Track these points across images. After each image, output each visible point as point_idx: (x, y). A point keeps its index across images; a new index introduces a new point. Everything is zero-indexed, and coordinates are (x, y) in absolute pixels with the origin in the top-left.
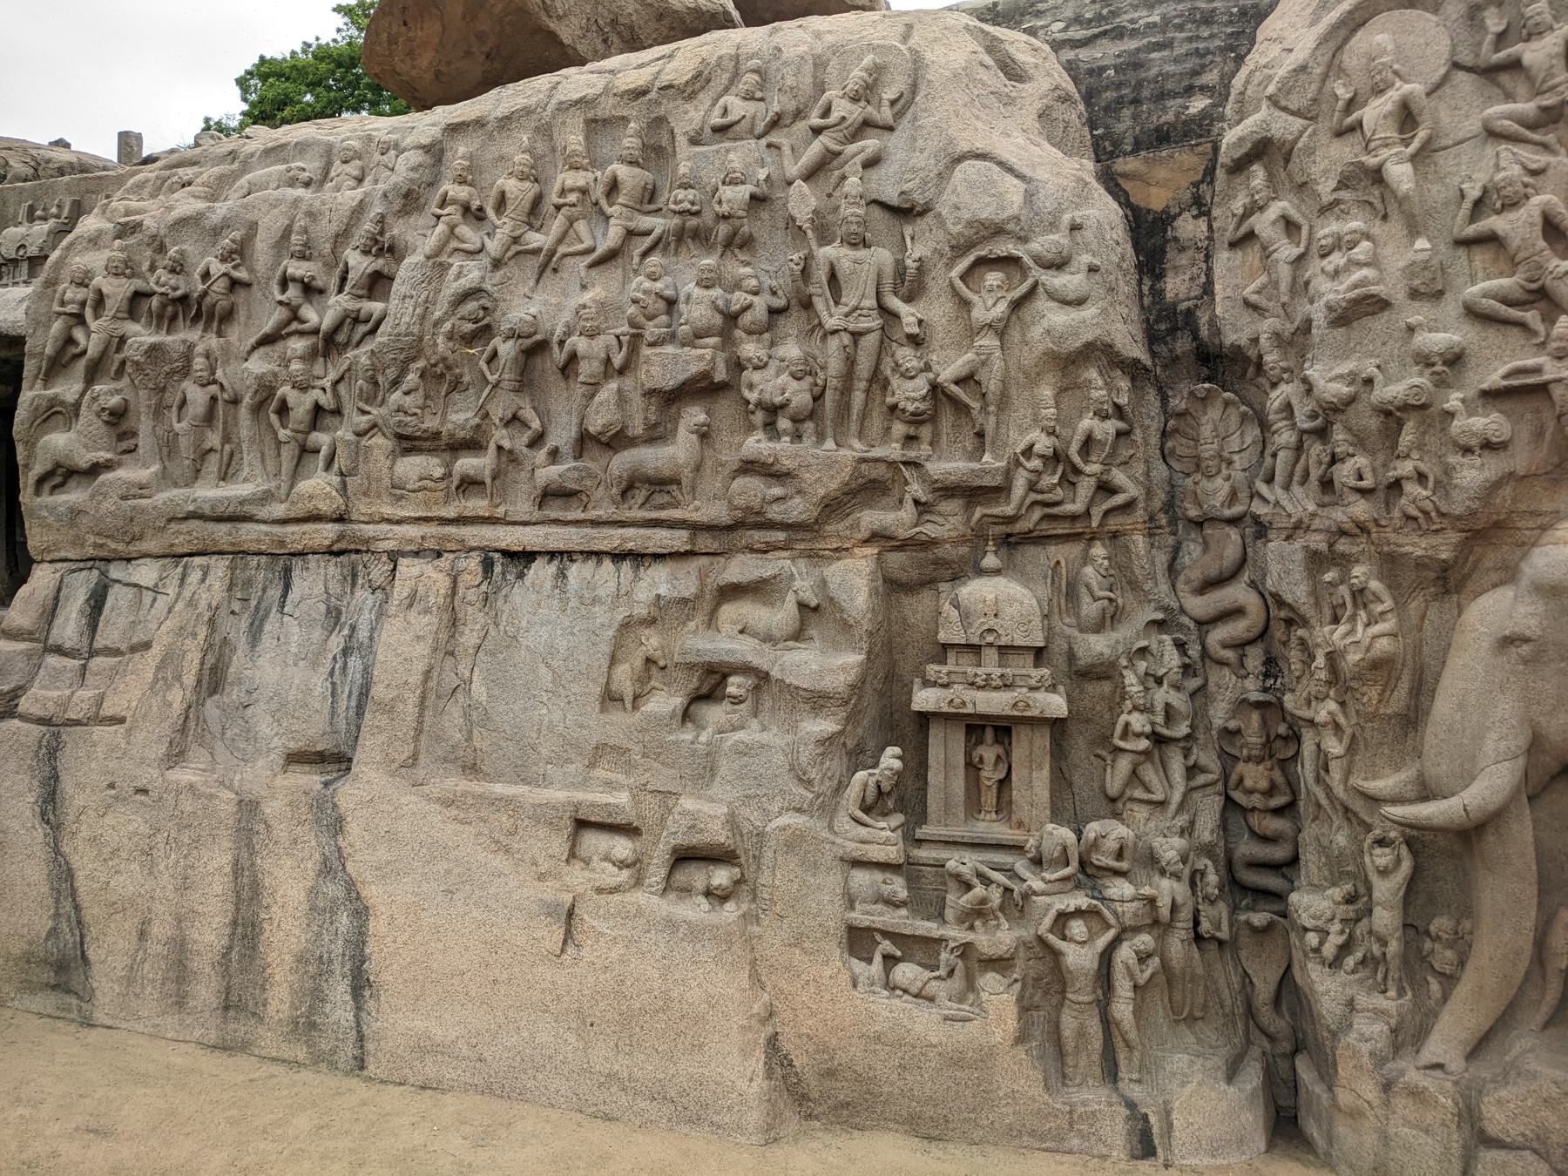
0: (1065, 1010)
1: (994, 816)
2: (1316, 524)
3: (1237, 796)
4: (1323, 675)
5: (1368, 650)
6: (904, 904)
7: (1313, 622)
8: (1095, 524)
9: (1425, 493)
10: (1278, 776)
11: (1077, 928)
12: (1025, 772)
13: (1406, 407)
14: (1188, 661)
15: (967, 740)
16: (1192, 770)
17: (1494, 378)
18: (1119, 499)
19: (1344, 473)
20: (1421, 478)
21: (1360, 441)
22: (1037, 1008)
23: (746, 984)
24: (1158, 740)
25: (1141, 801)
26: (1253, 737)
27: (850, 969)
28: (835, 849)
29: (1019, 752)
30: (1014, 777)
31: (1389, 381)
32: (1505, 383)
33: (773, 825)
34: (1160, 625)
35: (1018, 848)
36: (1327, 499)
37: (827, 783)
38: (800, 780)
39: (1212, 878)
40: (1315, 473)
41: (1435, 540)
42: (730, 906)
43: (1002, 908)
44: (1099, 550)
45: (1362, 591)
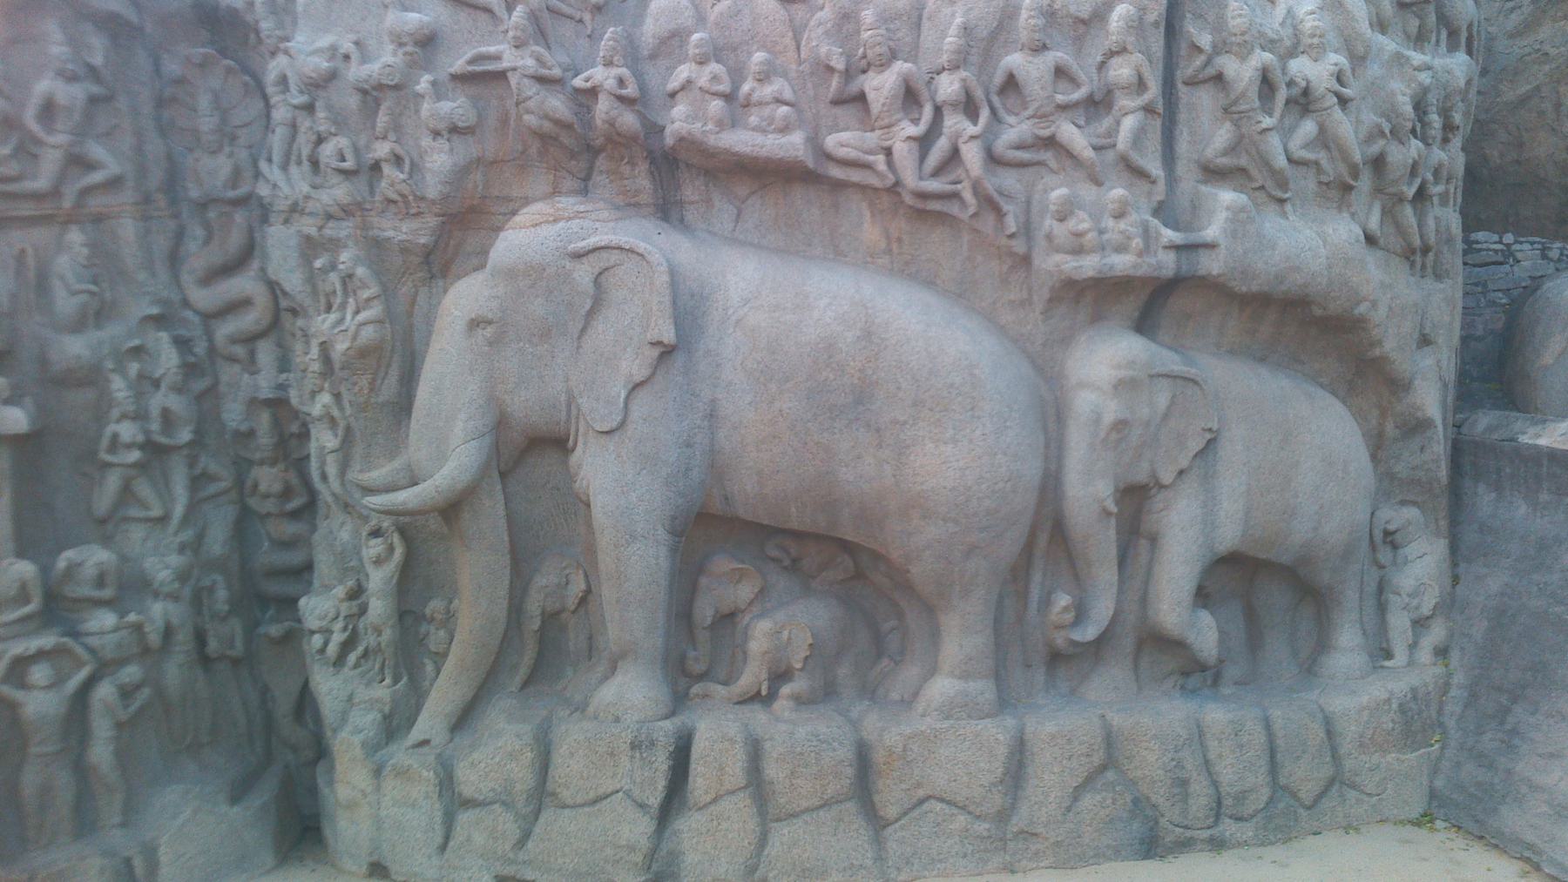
2: (310, 206)
3: (253, 502)
4: (316, 367)
5: (354, 338)
7: (311, 311)
8: (67, 204)
9: (402, 176)
10: (294, 480)
13: (380, 87)
14: (193, 359)
16: (198, 481)
17: (459, 65)
18: (97, 177)
19: (328, 151)
20: (398, 160)
21: (340, 122)
24: (155, 451)
25: (139, 520)
26: (265, 439)
31: (365, 59)
32: (470, 68)
34: (159, 321)
36: (318, 180)
39: (222, 594)
40: (305, 152)
41: (414, 224)
44: (75, 236)
45: (350, 276)
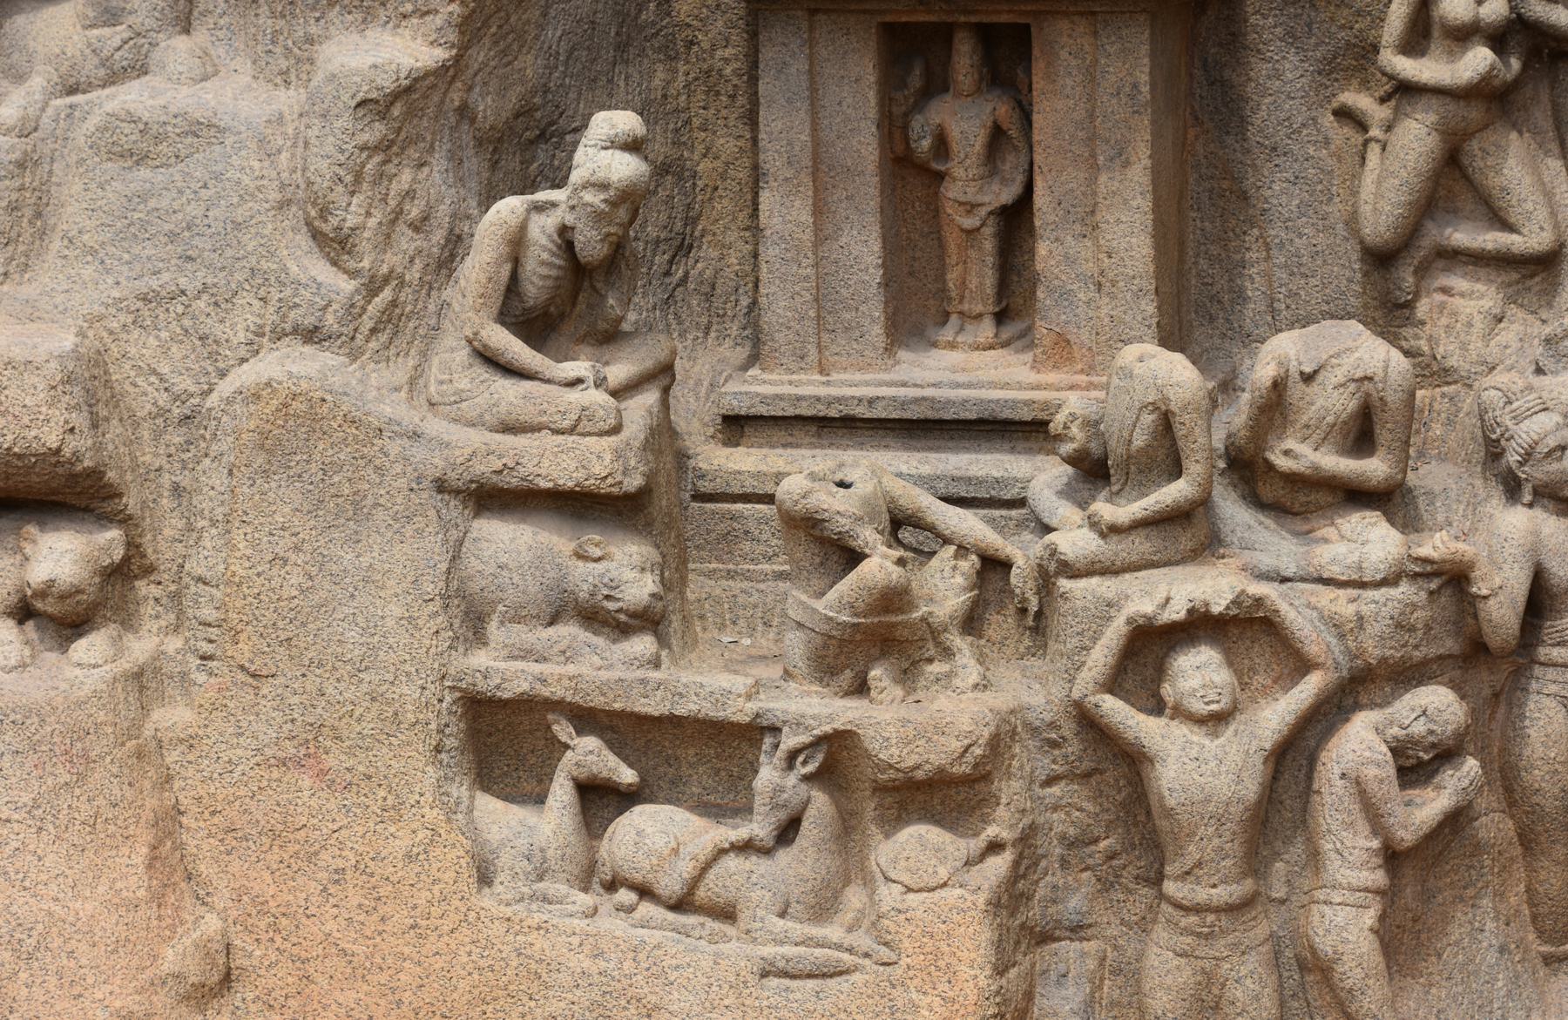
0: (1161, 933)
1: (986, 330)
6: (647, 620)
11: (1198, 672)
12: (1074, 178)
15: (890, 83)
22: (1078, 930)
23: (135, 884)
27: (472, 831)
28: (418, 453)
29: (1055, 110)
30: (1041, 199)
33: (226, 387)
35: (1028, 431)
37: (406, 241)
38: (316, 235)
42: (90, 647)
43: (971, 623)
